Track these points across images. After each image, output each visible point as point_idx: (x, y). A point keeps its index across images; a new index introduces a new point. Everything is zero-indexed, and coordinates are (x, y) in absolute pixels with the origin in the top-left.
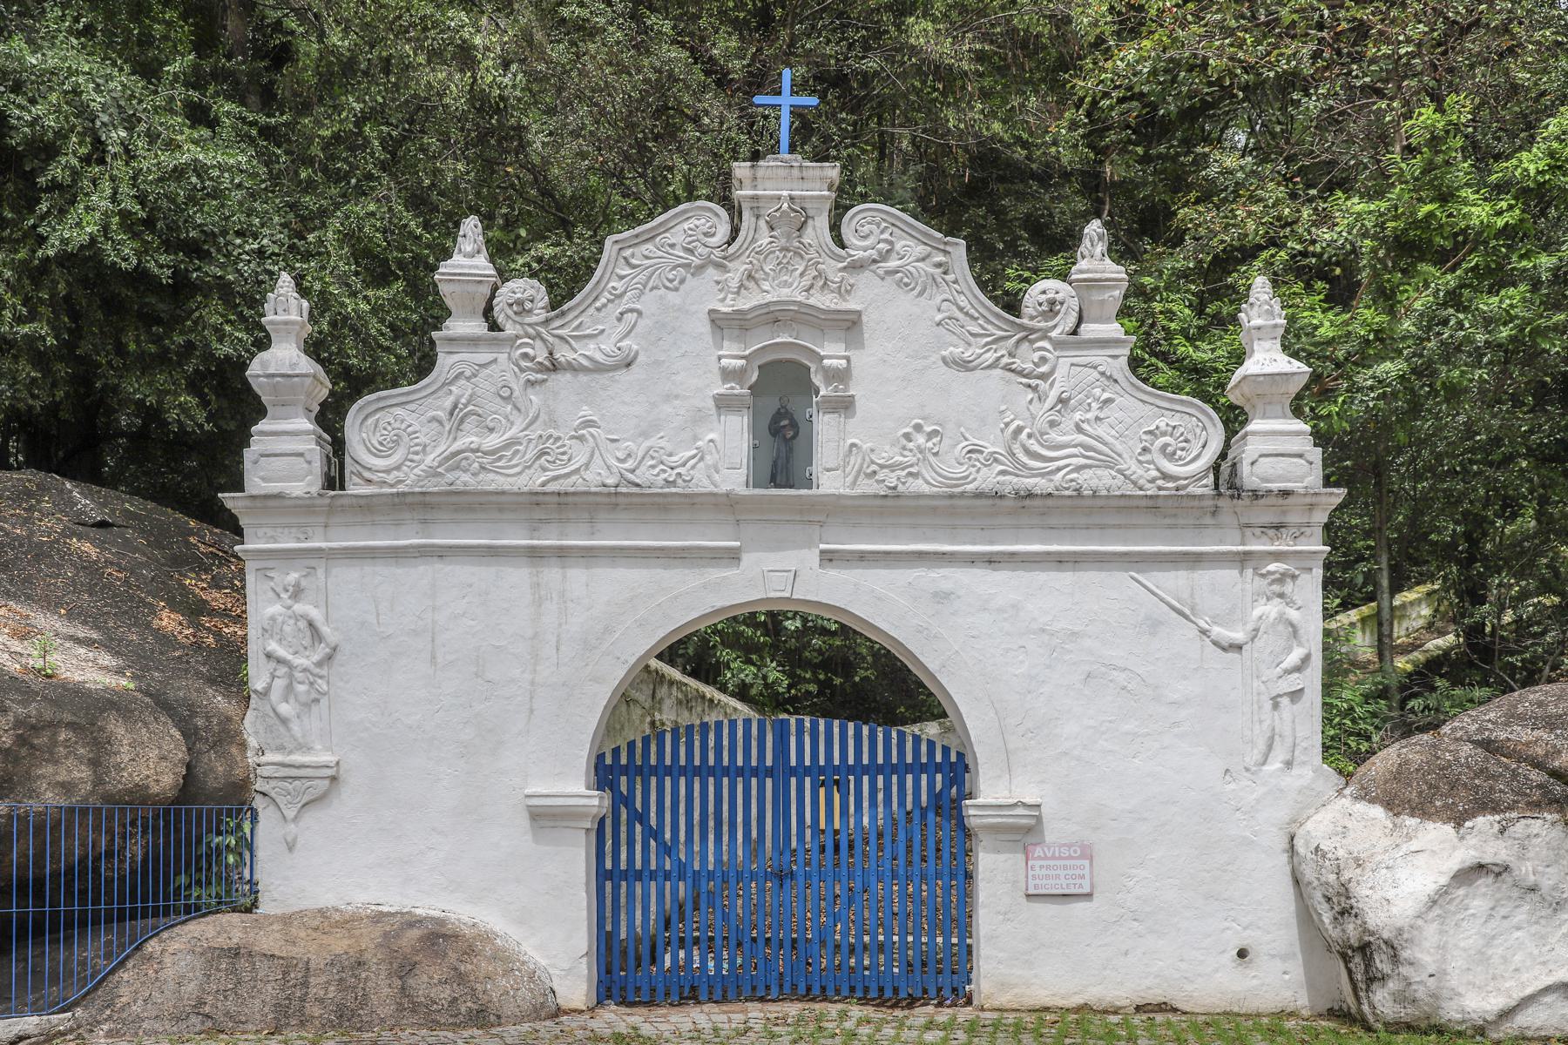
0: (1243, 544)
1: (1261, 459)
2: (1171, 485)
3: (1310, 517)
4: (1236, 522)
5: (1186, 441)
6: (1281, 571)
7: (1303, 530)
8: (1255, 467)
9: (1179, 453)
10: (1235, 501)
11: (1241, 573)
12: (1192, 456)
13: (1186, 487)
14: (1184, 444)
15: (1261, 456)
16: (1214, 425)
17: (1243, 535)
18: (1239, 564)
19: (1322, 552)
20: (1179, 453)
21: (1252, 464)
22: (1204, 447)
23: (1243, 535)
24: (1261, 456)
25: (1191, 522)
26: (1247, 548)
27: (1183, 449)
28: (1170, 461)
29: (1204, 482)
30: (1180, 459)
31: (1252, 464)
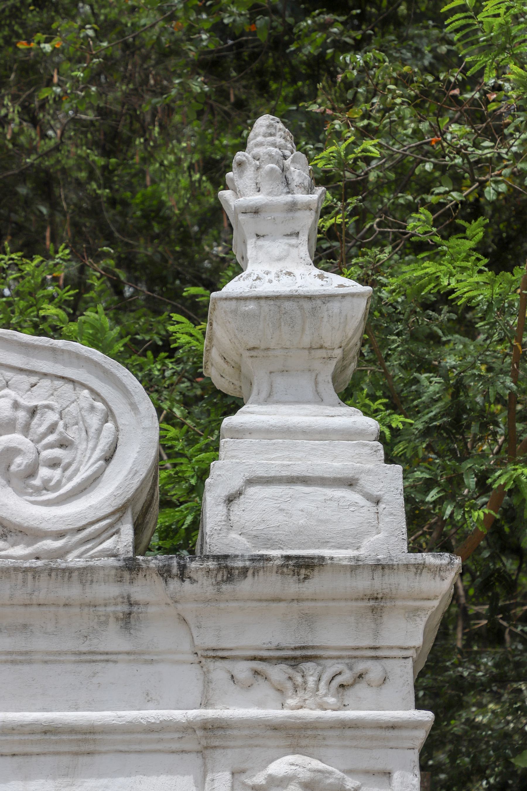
0: (205, 704)
1: (252, 491)
2: (20, 550)
3: (376, 634)
4: (187, 646)
5: (64, 444)
6: (305, 775)
7: (361, 666)
8: (237, 508)
9: (44, 472)
10: (174, 584)
11: (201, 782)
12: (77, 480)
13: (63, 553)
14: (57, 452)
15: (251, 482)
16: (134, 407)
17: (207, 682)
18: (195, 760)
19: (415, 725)
20: (44, 472)
21: (230, 500)
22: (108, 459)
23: (207, 682)
24: (251, 482)
25: (70, 644)
26: (210, 713)
27: (54, 464)
28: (21, 492)
29: (108, 544)
30: (46, 487)
31: (230, 500)
